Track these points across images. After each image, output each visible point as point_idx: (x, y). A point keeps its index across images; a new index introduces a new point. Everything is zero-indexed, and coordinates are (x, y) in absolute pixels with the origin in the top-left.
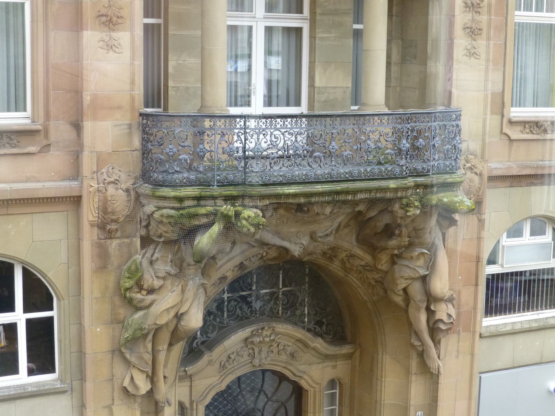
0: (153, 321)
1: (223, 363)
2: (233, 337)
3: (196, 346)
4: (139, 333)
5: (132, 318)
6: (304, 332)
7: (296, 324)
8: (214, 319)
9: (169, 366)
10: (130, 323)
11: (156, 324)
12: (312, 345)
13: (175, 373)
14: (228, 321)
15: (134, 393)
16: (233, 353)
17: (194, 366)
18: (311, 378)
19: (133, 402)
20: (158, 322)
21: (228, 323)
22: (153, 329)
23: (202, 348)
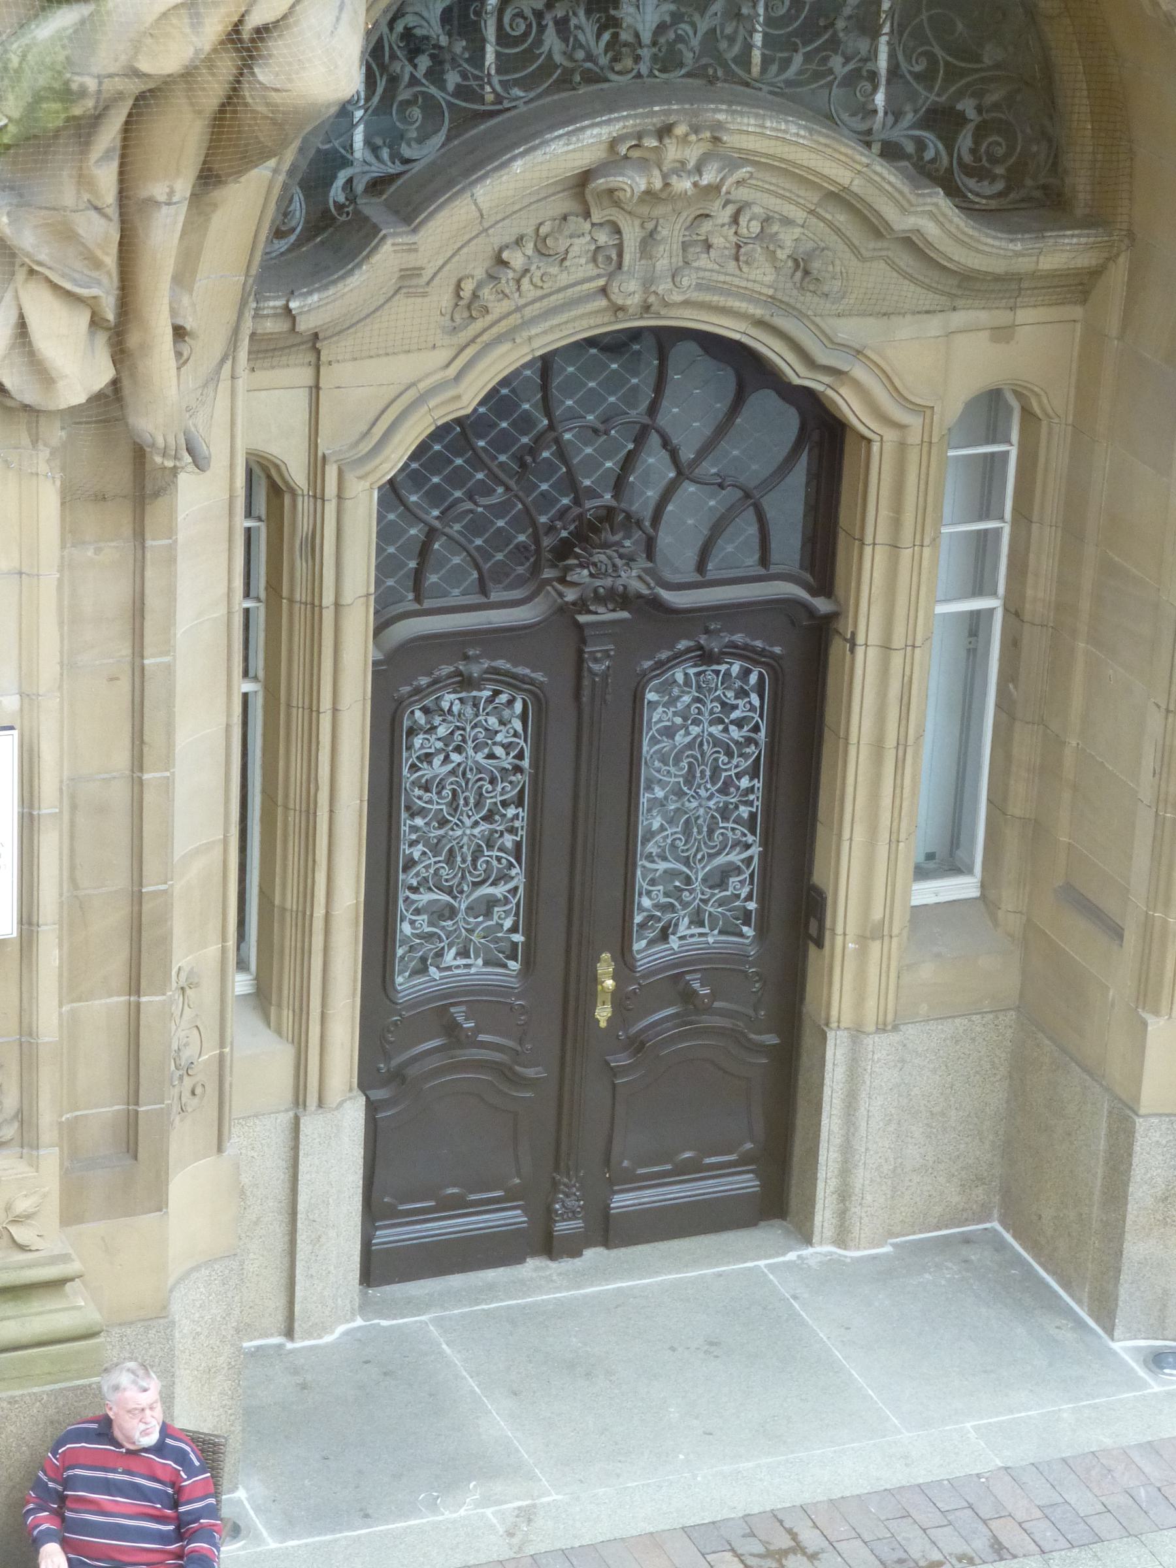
0: (123, 57)
1: (468, 287)
2: (518, 166)
3: (341, 199)
4: (53, 115)
5: (25, 41)
6: (862, 157)
7: (829, 119)
8: (435, 75)
9: (202, 283)
10: (15, 61)
11: (136, 73)
12: (902, 223)
13: (230, 315)
14: (498, 88)
15: (28, 399)
16: (519, 241)
17: (331, 291)
18: (887, 378)
19: (25, 440)
20: (144, 66)
21: (499, 99)
22: (119, 96)
23: (372, 208)
